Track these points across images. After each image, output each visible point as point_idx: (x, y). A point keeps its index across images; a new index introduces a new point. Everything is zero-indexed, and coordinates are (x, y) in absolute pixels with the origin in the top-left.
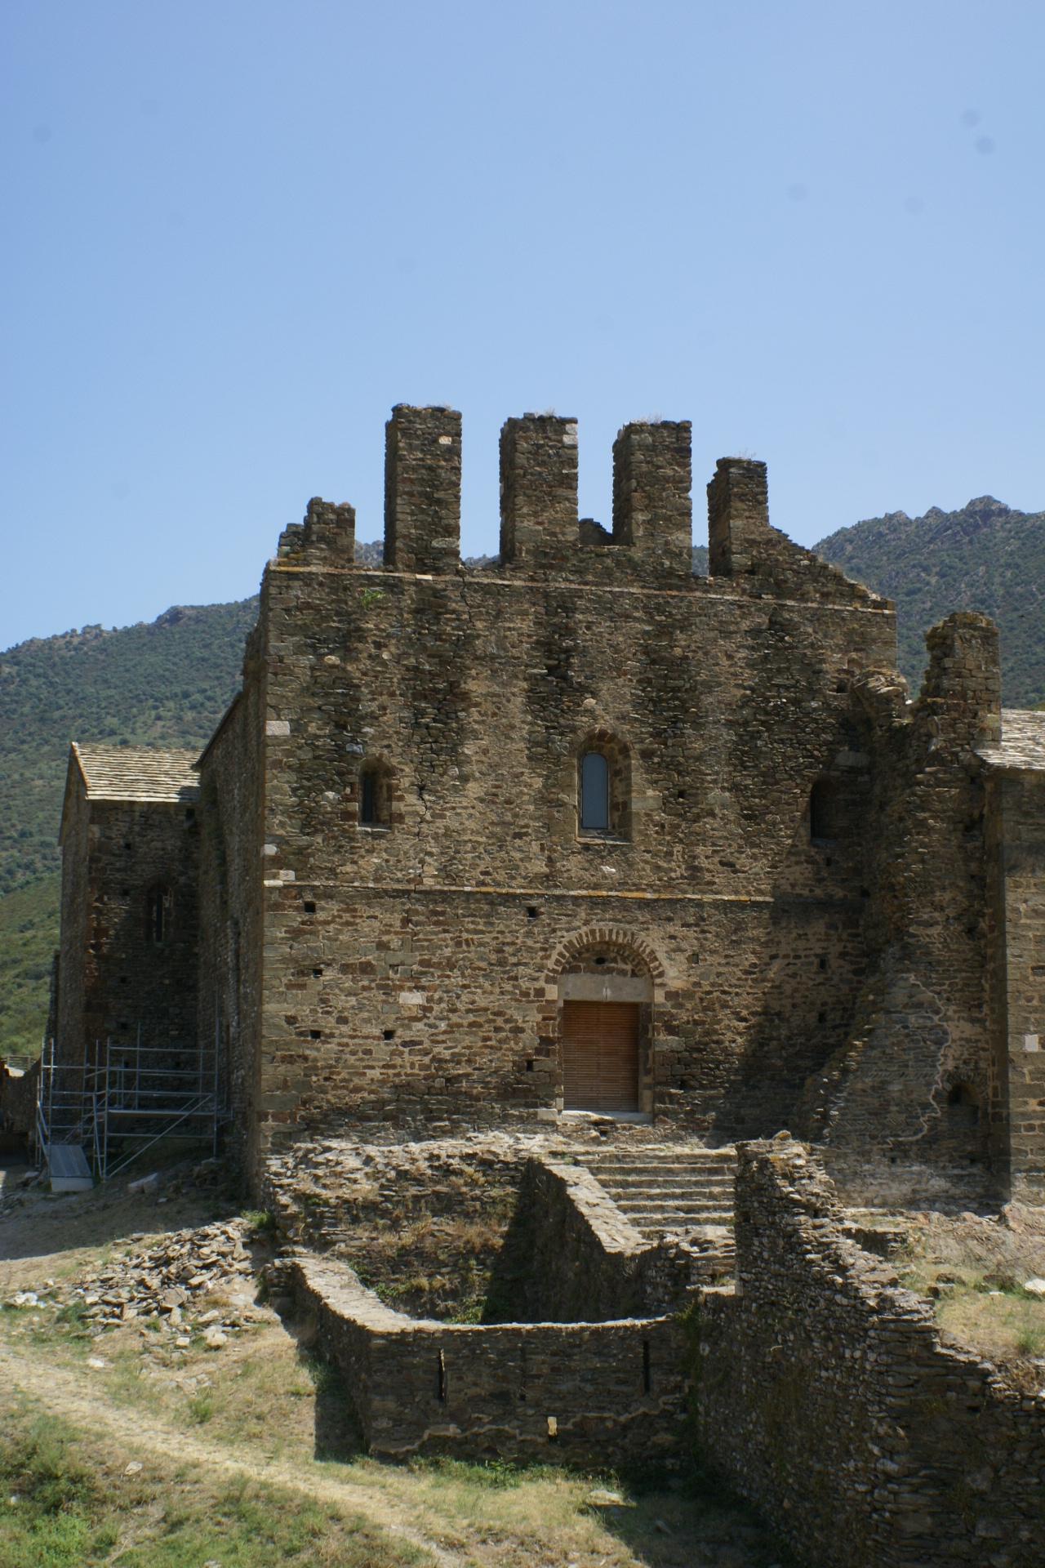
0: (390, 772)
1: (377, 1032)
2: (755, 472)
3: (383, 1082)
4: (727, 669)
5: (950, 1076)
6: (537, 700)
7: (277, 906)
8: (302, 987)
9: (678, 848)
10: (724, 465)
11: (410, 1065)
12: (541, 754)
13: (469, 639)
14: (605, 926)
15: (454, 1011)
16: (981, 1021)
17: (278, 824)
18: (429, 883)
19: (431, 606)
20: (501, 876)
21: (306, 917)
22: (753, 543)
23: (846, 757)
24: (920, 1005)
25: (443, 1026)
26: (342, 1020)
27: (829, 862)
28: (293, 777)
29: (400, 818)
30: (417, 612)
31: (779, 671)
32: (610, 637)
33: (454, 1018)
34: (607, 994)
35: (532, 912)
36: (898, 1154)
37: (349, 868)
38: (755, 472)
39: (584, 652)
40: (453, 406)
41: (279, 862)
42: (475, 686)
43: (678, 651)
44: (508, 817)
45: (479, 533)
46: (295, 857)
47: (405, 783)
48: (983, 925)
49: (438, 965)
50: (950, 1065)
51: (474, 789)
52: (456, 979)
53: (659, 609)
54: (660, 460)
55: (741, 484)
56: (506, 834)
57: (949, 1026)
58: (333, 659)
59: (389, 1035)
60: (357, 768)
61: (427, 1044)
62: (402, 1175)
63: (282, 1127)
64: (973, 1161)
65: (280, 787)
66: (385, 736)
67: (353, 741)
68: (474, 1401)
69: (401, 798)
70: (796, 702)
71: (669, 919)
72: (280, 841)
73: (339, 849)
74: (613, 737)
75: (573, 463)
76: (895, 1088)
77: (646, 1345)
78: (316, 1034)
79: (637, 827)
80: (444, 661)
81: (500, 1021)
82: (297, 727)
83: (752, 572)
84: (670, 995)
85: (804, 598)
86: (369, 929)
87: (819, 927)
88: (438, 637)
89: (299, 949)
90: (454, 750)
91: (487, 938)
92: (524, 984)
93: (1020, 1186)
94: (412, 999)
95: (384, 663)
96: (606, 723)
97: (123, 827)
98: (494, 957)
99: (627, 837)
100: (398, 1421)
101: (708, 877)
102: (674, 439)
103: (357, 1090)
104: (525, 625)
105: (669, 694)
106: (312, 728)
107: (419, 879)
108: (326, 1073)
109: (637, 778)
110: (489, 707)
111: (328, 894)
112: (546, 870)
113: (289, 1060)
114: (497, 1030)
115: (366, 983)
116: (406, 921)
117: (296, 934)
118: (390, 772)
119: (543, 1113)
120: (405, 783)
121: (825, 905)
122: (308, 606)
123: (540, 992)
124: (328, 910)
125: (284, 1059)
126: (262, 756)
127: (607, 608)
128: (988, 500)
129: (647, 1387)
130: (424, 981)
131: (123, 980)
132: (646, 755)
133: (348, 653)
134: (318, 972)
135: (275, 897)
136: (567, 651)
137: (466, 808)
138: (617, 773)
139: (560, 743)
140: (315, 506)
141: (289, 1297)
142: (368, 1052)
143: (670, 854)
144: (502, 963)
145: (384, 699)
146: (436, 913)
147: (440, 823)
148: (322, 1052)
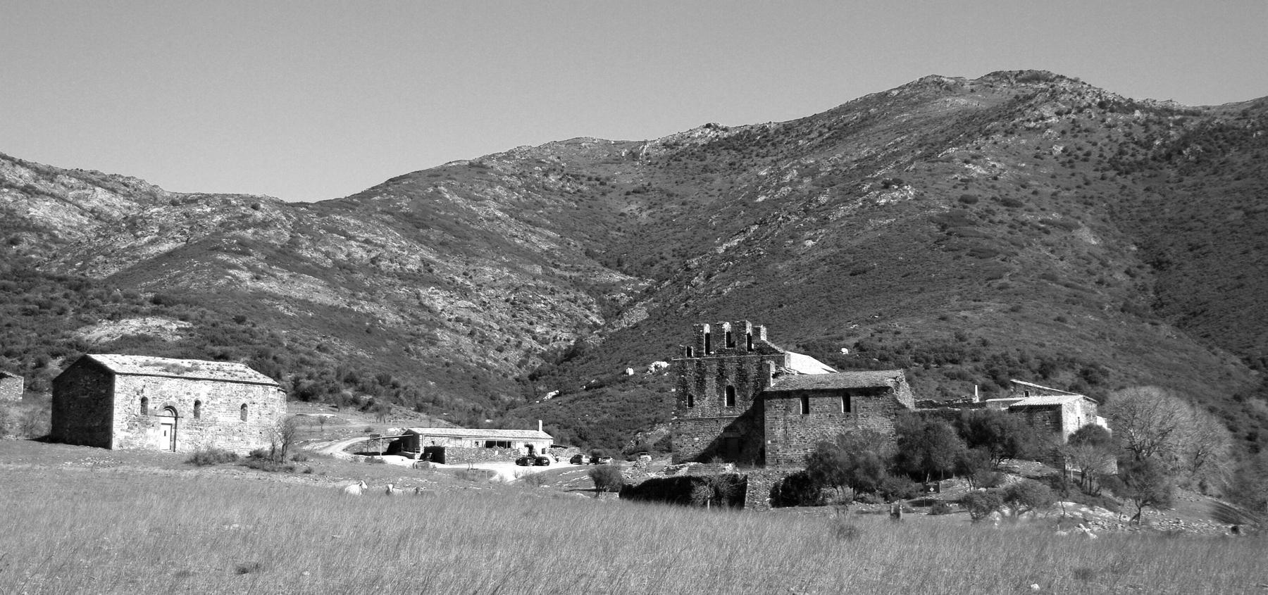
12: (719, 391)
42: (707, 379)
56: (713, 406)
127: (730, 360)
137: (706, 403)
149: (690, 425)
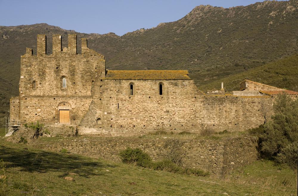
1: (35, 114)
3: (35, 120)
7: (22, 99)
9: (74, 90)
12: (56, 79)
13: (46, 65)
14: (64, 100)
15: (44, 111)
20: (51, 94)
21: (25, 100)
25: (43, 113)
26: (30, 113)
29: (37, 88)
50: (97, 116)
51: (47, 83)
52: (45, 107)
58: (29, 68)
59: (36, 114)
61: (41, 115)
65: (22, 84)
66: (35, 77)
69: (38, 85)
71: (72, 99)
76: (90, 119)
81: (50, 112)
82: (25, 77)
84: (72, 108)
86: (33, 102)
90: (45, 78)
92: (53, 108)
94: (39, 110)
96: (64, 75)
101: (78, 93)
106: (26, 77)
108: (28, 119)
112: (56, 93)
114: (50, 113)
115: (33, 108)
116: (38, 100)
120: (38, 83)
123: (55, 109)
127: (64, 60)
135: (22, 98)
139: (58, 78)
142: (33, 117)
143: (73, 91)
144: (51, 106)
145: (36, 73)
146: (42, 99)
149: (35, 100)
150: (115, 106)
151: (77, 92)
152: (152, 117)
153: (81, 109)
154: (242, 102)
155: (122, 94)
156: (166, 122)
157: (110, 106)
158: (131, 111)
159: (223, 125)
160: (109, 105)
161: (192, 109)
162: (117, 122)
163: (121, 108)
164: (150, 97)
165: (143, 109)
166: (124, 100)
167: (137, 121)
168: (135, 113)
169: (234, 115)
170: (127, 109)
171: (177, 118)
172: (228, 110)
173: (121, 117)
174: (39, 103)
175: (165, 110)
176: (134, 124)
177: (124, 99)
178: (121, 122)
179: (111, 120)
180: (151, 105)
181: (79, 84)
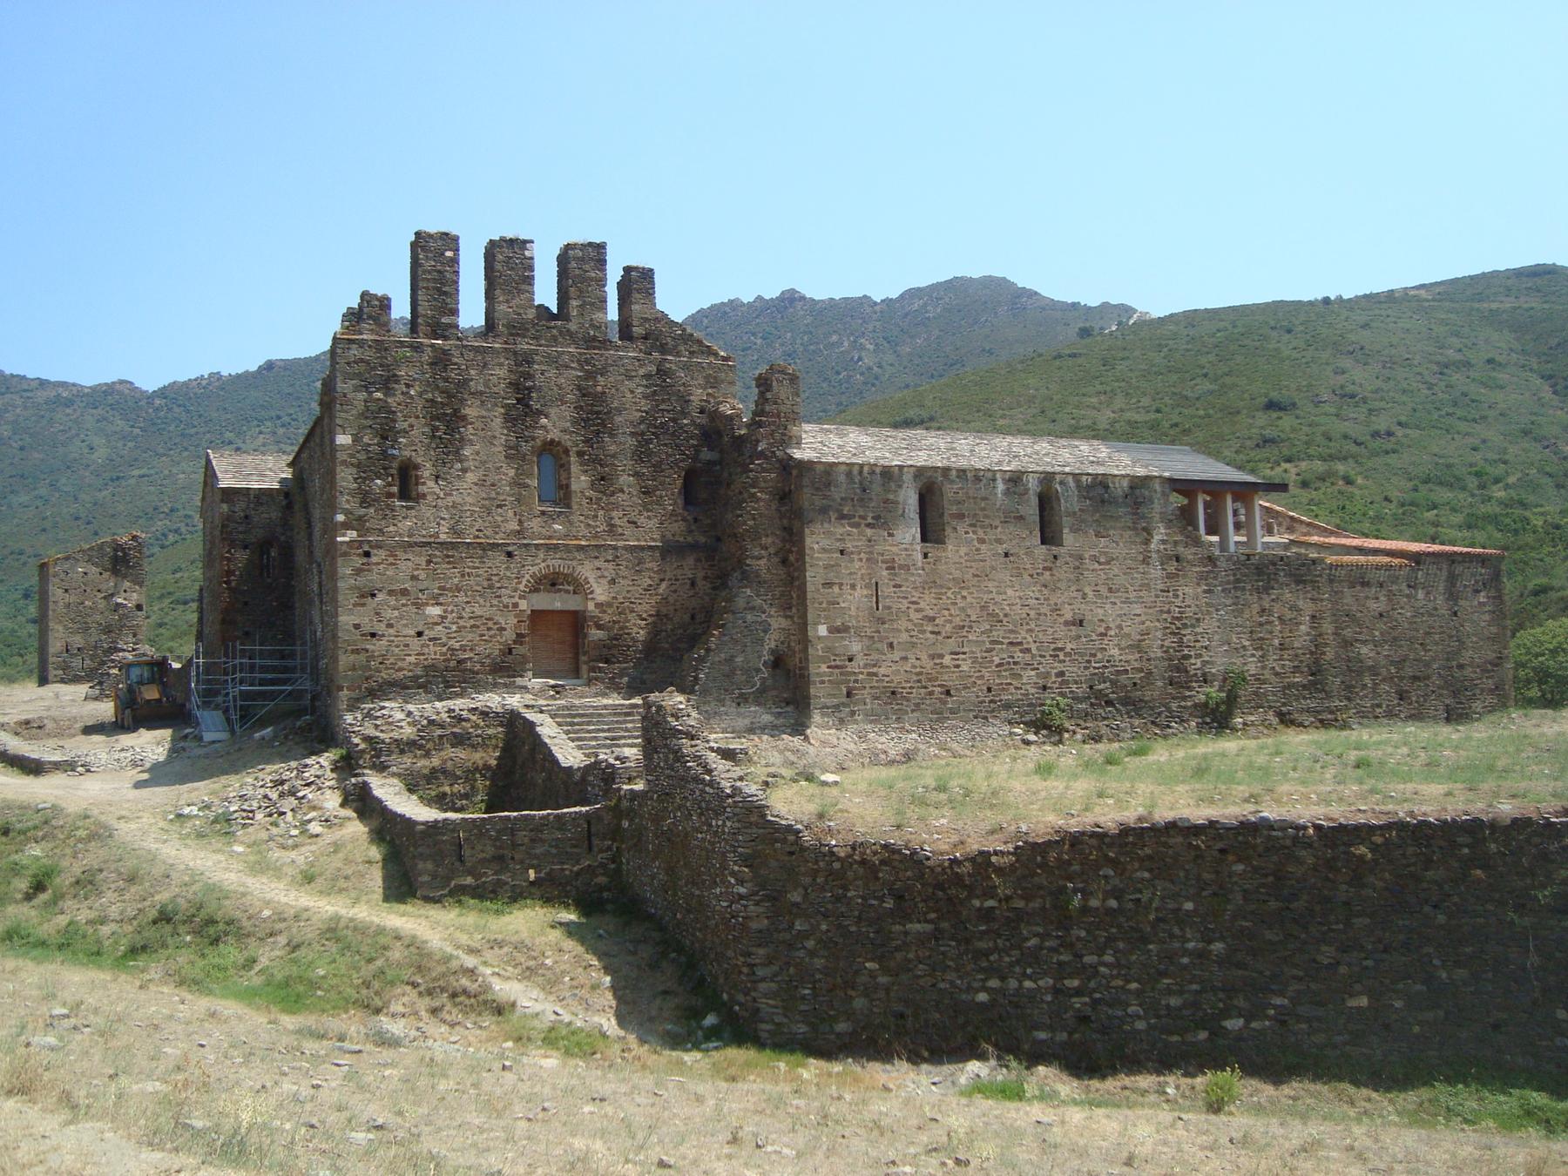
0: (417, 467)
1: (412, 633)
2: (647, 275)
3: (416, 665)
4: (630, 400)
5: (772, 652)
6: (510, 420)
7: (345, 554)
8: (363, 605)
9: (601, 513)
10: (628, 270)
11: (434, 653)
13: (466, 382)
14: (556, 563)
16: (791, 617)
17: (344, 501)
18: (443, 537)
19: (441, 360)
20: (489, 532)
21: (365, 560)
22: (646, 320)
23: (706, 454)
24: (753, 608)
25: (454, 628)
26: (390, 626)
27: (696, 520)
28: (354, 470)
29: (424, 496)
30: (432, 364)
31: (663, 401)
32: (556, 380)
33: (461, 623)
34: (558, 605)
35: (510, 555)
36: (742, 700)
37: (392, 528)
38: (647, 275)
39: (540, 389)
40: (454, 232)
41: (346, 526)
42: (471, 411)
43: (599, 389)
44: (493, 495)
45: (471, 311)
46: (357, 523)
47: (427, 474)
48: (792, 558)
49: (450, 590)
50: (773, 645)
51: (471, 477)
52: (462, 598)
53: (587, 362)
54: (587, 267)
55: (638, 282)
56: (491, 506)
57: (772, 621)
58: (379, 395)
59: (420, 634)
60: (395, 465)
62: (431, 722)
63: (353, 695)
64: (788, 704)
65: (346, 478)
66: (414, 444)
67: (393, 447)
68: (483, 861)
70: (674, 420)
72: (347, 512)
73: (385, 517)
74: (559, 443)
75: (531, 268)
76: (739, 659)
77: (589, 823)
78: (373, 635)
79: (575, 500)
80: (450, 396)
81: (490, 624)
83: (645, 338)
85: (678, 354)
86: (406, 567)
87: (690, 561)
88: (446, 380)
89: (361, 581)
91: (481, 572)
92: (505, 600)
93: (817, 717)
94: (435, 611)
95: (411, 397)
96: (554, 434)
97: (243, 505)
98: (485, 584)
99: (568, 506)
100: (434, 877)
102: (596, 254)
103: (401, 669)
104: (502, 372)
105: (594, 415)
106: (366, 440)
107: (437, 535)
109: (575, 468)
110: (479, 425)
111: (379, 546)
113: (356, 652)
116: (429, 562)
117: (358, 572)
118: (417, 467)
119: (519, 681)
120: (427, 474)
121: (694, 547)
122: (362, 360)
123: (516, 605)
124: (378, 556)
125: (353, 651)
126: (333, 457)
127: (553, 361)
128: (793, 291)
129: (590, 849)
130: (441, 600)
131: (246, 603)
132: (580, 454)
133: (388, 391)
134: (373, 595)
135: (344, 548)
136: (529, 389)
137: (466, 489)
138: (562, 466)
139: (525, 447)
140: (365, 295)
141: (362, 802)
144: (490, 587)
147: (449, 499)
148: (377, 646)
149: (411, 563)
150: (860, 592)
151: (613, 526)
152: (1017, 649)
153: (638, 608)
154: (1331, 581)
155: (890, 535)
156: (1073, 671)
157: (841, 595)
158: (933, 619)
159: (1273, 679)
160: (836, 589)
161: (1169, 612)
162: (875, 674)
163: (888, 602)
164: (1006, 555)
165: (983, 608)
166: (901, 567)
167: (958, 666)
168: (948, 627)
169: (1308, 634)
170: (917, 611)
171: (1115, 652)
172: (1289, 615)
173: (891, 645)
174: (434, 576)
175: (1068, 616)
176: (950, 679)
177: (899, 561)
178: (892, 670)
179: (851, 667)
180: (1014, 594)
181: (625, 480)
